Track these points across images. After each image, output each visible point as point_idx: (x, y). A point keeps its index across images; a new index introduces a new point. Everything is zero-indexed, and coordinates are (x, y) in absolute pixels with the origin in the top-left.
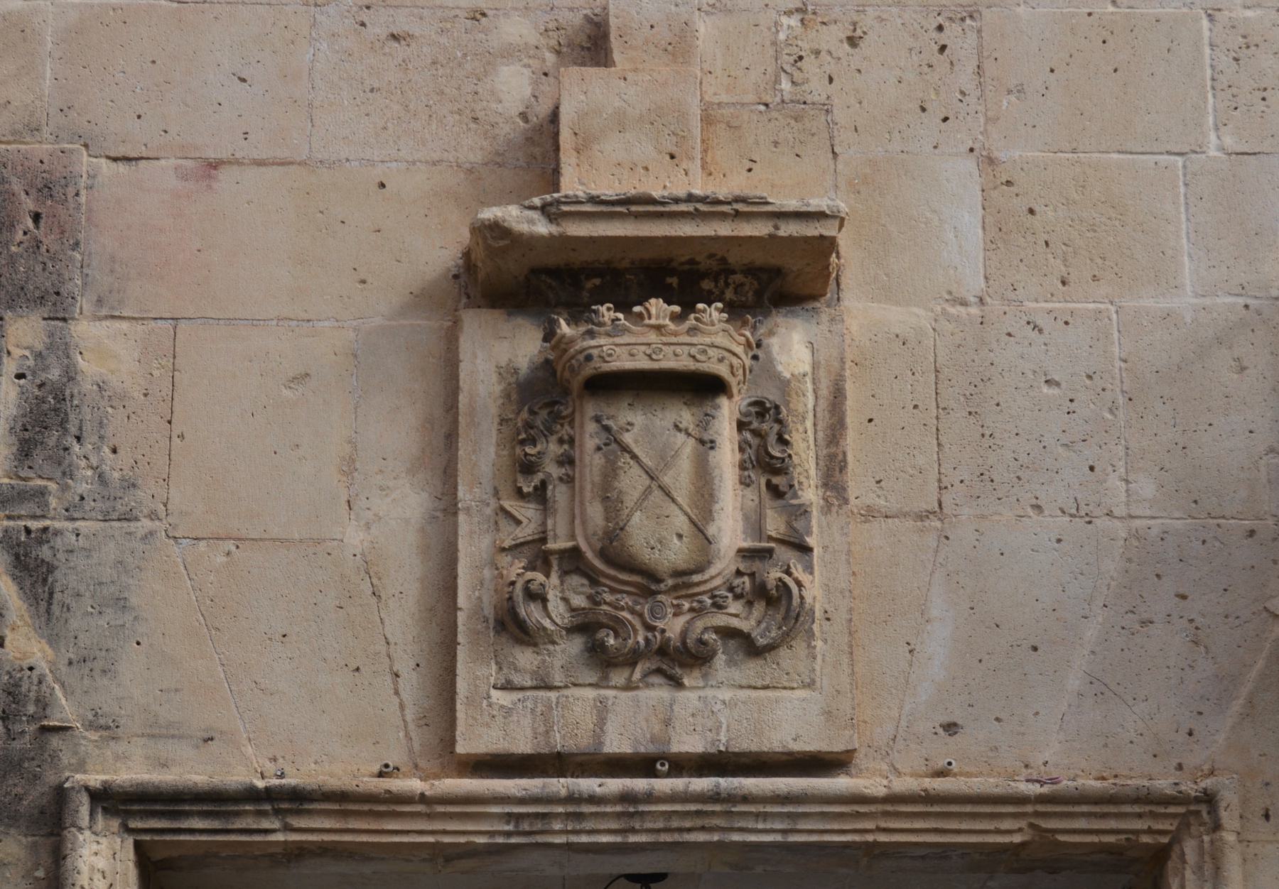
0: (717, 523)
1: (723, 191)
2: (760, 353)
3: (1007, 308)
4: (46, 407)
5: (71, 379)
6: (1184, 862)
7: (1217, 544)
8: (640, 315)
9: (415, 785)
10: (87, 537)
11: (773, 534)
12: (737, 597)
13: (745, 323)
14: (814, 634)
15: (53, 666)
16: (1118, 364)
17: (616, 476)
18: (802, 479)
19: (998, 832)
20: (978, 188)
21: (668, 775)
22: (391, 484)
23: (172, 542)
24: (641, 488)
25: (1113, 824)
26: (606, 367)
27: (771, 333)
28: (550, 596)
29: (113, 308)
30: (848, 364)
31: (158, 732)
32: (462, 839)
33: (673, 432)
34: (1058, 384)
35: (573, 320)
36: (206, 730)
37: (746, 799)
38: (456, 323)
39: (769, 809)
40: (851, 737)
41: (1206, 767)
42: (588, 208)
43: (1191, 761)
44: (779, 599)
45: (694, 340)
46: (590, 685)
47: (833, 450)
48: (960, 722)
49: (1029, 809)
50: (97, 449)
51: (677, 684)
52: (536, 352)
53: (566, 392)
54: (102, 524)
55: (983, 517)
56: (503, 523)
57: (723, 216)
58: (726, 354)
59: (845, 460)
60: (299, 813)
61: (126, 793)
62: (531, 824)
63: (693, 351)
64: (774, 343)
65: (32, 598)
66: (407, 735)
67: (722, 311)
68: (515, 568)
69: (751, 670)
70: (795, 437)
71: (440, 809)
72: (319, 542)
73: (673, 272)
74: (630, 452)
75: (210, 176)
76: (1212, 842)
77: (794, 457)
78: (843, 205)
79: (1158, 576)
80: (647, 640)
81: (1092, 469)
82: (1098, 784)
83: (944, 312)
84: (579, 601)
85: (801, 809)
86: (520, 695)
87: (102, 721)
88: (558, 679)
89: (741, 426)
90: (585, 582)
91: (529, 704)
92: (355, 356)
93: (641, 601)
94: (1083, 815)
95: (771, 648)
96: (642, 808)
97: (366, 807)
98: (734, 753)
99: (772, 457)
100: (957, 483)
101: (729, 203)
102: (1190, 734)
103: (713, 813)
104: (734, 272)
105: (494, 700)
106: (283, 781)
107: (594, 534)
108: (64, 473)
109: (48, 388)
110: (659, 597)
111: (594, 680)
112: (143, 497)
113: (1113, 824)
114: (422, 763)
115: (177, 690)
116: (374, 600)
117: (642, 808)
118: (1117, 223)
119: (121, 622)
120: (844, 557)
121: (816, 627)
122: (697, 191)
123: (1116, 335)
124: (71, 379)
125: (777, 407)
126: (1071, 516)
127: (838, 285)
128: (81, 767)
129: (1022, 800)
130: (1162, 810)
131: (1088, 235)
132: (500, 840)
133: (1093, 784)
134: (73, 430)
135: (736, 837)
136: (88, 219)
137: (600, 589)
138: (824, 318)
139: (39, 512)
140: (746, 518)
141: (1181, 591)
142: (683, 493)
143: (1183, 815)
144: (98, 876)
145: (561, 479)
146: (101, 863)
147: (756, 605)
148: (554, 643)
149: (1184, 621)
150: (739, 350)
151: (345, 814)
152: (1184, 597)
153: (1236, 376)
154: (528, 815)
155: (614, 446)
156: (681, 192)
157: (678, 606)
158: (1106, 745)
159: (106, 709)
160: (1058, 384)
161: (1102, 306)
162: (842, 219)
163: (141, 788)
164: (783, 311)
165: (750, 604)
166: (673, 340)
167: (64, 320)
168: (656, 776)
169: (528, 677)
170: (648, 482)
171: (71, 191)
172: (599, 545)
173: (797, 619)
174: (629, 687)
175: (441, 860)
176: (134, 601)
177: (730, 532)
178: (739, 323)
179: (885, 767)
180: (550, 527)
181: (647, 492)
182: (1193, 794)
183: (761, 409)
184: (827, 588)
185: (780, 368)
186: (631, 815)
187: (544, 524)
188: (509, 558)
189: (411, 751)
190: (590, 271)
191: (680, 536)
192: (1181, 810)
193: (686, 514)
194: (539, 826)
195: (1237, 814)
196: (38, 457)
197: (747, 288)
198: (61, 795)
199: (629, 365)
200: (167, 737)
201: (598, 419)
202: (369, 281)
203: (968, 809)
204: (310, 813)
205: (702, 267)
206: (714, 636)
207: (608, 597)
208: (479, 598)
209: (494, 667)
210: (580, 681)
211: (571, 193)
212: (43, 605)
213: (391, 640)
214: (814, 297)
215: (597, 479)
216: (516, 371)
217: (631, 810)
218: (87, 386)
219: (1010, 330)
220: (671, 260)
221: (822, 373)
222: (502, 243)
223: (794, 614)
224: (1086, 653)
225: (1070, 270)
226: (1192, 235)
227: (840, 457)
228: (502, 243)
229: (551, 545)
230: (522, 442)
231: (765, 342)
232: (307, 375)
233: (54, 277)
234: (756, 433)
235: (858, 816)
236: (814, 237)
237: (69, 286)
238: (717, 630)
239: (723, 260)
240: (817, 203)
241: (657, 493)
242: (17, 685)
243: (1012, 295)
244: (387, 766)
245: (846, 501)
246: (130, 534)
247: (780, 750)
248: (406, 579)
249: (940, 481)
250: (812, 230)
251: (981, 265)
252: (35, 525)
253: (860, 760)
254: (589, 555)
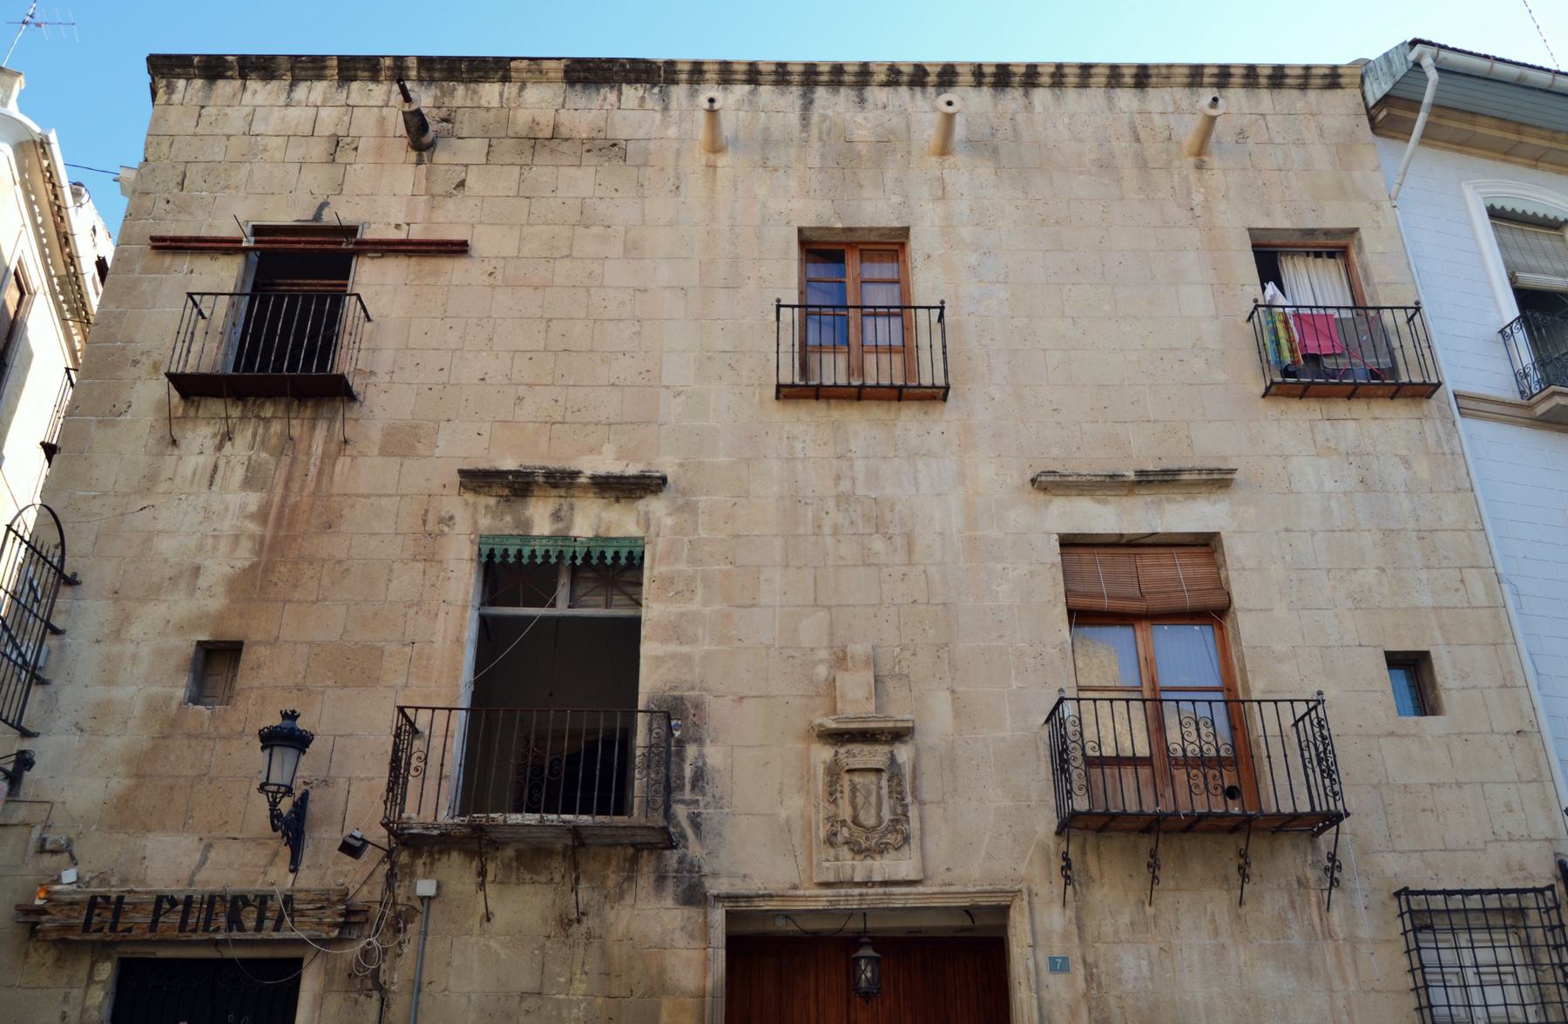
177: (886, 815)
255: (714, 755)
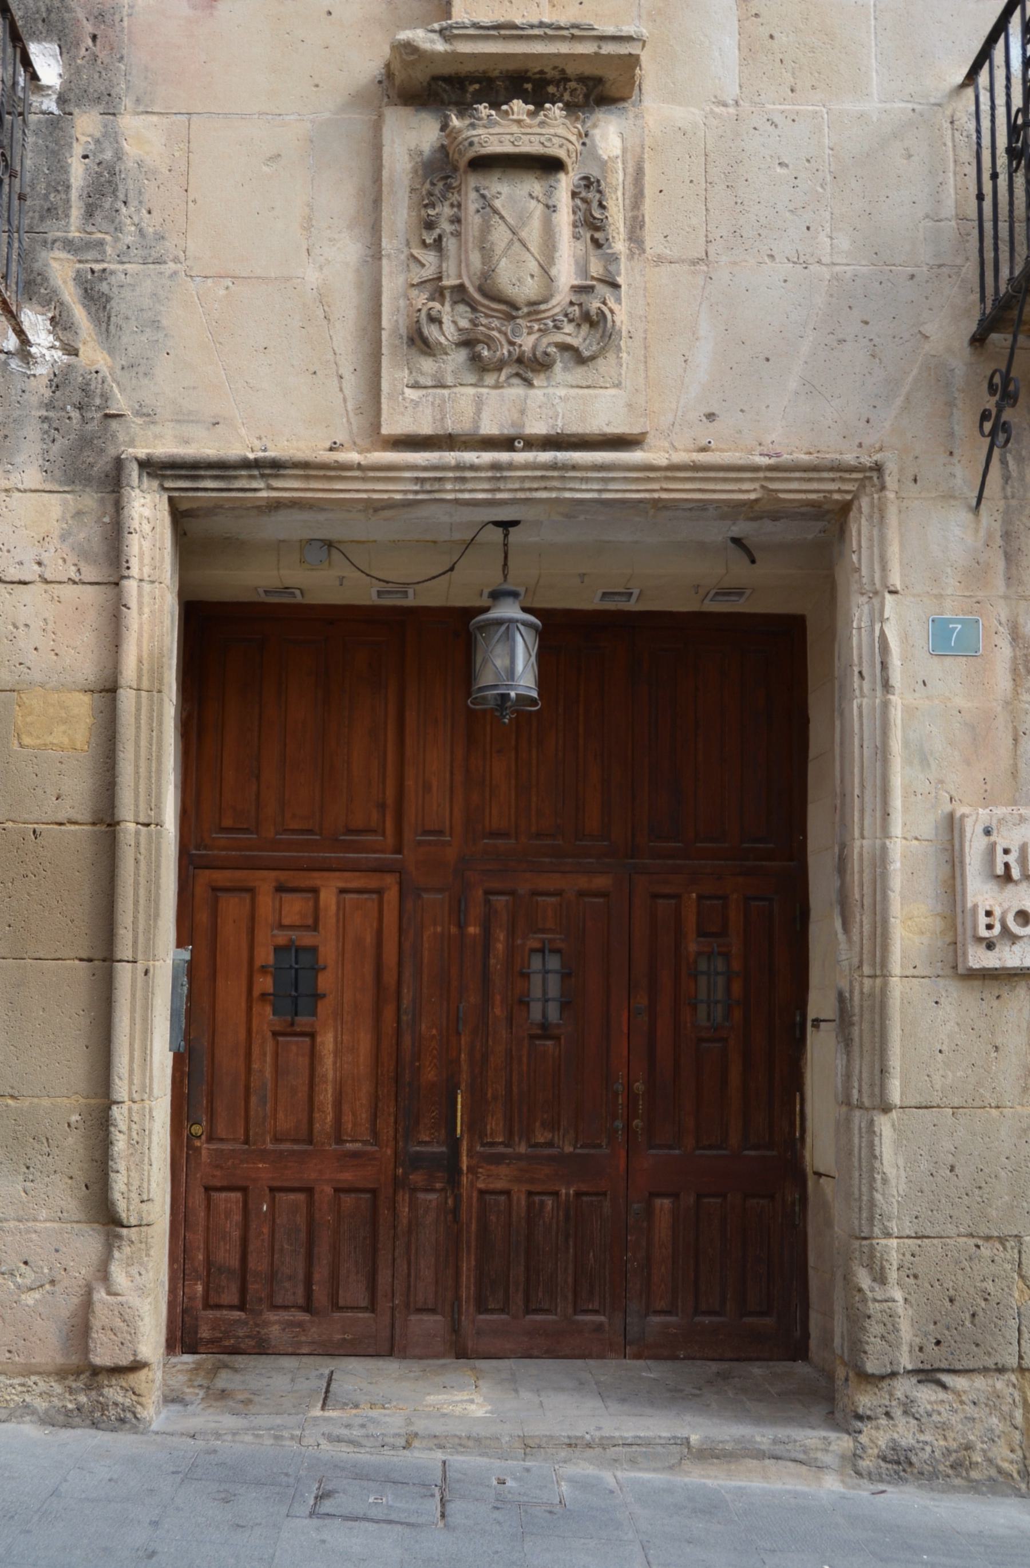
0: (557, 266)
1: (563, 18)
2: (587, 141)
3: (753, 109)
4: (103, 179)
5: (119, 159)
6: (861, 513)
7: (890, 284)
8: (506, 112)
9: (353, 457)
10: (132, 276)
11: (595, 275)
12: (571, 321)
13: (577, 119)
14: (621, 349)
15: (111, 369)
16: (827, 151)
17: (489, 232)
18: (615, 235)
19: (740, 491)
20: (736, 19)
21: (523, 450)
22: (336, 237)
23: (189, 279)
24: (506, 241)
25: (815, 486)
26: (484, 151)
27: (595, 126)
28: (444, 320)
29: (147, 106)
30: (647, 149)
31: (183, 418)
32: (385, 496)
33: (528, 199)
34: (787, 166)
35: (461, 115)
36: (214, 417)
37: (574, 467)
38: (380, 116)
39: (590, 474)
40: (645, 423)
41: (877, 446)
42: (471, 32)
43: (867, 441)
44: (598, 322)
45: (543, 131)
46: (471, 385)
47: (636, 213)
48: (716, 412)
49: (761, 475)
50: (138, 211)
51: (529, 383)
52: (435, 139)
53: (455, 169)
54: (142, 266)
55: (735, 263)
56: (413, 266)
57: (563, 38)
58: (565, 142)
59: (643, 221)
60: (277, 476)
61: (162, 463)
62: (431, 485)
63: (543, 139)
64: (596, 133)
65: (97, 321)
66: (348, 421)
67: (562, 109)
68: (420, 299)
69: (579, 374)
70: (610, 203)
71: (371, 474)
72: (288, 279)
73: (528, 80)
74: (499, 214)
75: (212, 7)
76: (879, 498)
77: (610, 218)
78: (644, 31)
79: (850, 307)
80: (509, 352)
81: (808, 228)
82: (806, 457)
83: (712, 111)
84: (464, 323)
85: (611, 475)
86: (424, 392)
87: (145, 410)
88: (449, 380)
89: (574, 195)
90: (468, 309)
91: (430, 399)
92: (312, 141)
93: (506, 323)
94: (797, 479)
95: (593, 358)
96: (506, 474)
97: (322, 473)
98: (567, 435)
99: (595, 218)
100: (718, 238)
101: (567, 29)
102: (868, 422)
103: (553, 477)
104: (570, 80)
105: (406, 395)
106: (267, 454)
107: (475, 274)
108: (116, 229)
109: (104, 165)
110: (518, 321)
111: (473, 381)
112: (170, 246)
113: (815, 486)
114: (358, 441)
115: (194, 388)
116: (325, 322)
117: (506, 474)
118: (829, 46)
119: (155, 338)
120: (642, 292)
121: (622, 343)
122: (546, 20)
123: (826, 129)
124: (119, 159)
125: (598, 181)
126: (794, 263)
127: (640, 90)
128: (132, 443)
129: (756, 469)
130: (847, 476)
131: (810, 55)
132: (411, 496)
133: (803, 458)
134: (122, 196)
135: (568, 495)
136: (129, 39)
137: (478, 315)
138: (631, 115)
139: (100, 258)
140: (577, 263)
141: (865, 318)
142: (533, 242)
143: (862, 479)
144: (145, 521)
145: (452, 233)
146: (147, 512)
147: (583, 327)
148: (446, 354)
149: (866, 340)
150: (573, 138)
151: (307, 477)
152: (866, 323)
153: (905, 161)
154: (429, 479)
155: (488, 209)
156: (535, 21)
157: (530, 327)
158: (812, 430)
159: (147, 402)
160: (787, 166)
161: (817, 108)
162: (644, 42)
163: (172, 459)
164: (604, 109)
165: (579, 325)
166: (529, 131)
167: (114, 114)
168: (515, 451)
169: (429, 379)
170: (511, 236)
171: (117, 18)
172: (477, 283)
173: (610, 337)
174: (497, 386)
175: (371, 511)
176: (165, 322)
177: (566, 274)
178: (573, 118)
179: (667, 445)
180: (444, 269)
181: (511, 242)
182: (869, 465)
183: (588, 182)
184: (630, 314)
185: (600, 152)
186: (498, 479)
187: (440, 266)
188: (416, 292)
189: (351, 432)
190: (472, 78)
191: (532, 276)
192: (860, 476)
193: (537, 260)
194: (436, 487)
195: (896, 479)
196: (98, 218)
197: (578, 92)
198: (119, 463)
199: (498, 149)
200: (188, 421)
201: (477, 190)
202: (321, 85)
203: (721, 475)
204: (284, 476)
205: (548, 76)
206: (554, 350)
207: (484, 321)
208: (397, 321)
209: (406, 371)
210: (464, 382)
211: (459, 20)
212: (104, 325)
213: (338, 352)
214: (623, 99)
215: (477, 234)
216: (421, 153)
217: (498, 475)
218: (130, 164)
219: (755, 125)
220: (527, 71)
221: (629, 155)
222: (412, 58)
223: (608, 334)
224: (801, 363)
225: (797, 81)
226: (879, 56)
227: (640, 218)
228: (412, 58)
229: (445, 283)
230: (426, 206)
231: (591, 132)
232: (279, 155)
233: (107, 82)
234: (584, 200)
235: (649, 479)
236: (625, 55)
237: (117, 89)
238: (557, 345)
239: (563, 71)
240: (628, 30)
241: (517, 244)
242: (88, 384)
243: (756, 99)
244: (335, 443)
245: (644, 251)
246: (161, 273)
247: (597, 432)
248: (347, 307)
249: (706, 236)
250: (623, 49)
251: (737, 77)
252: (97, 267)
253: (650, 440)
254: (471, 290)
255: (143, 138)
